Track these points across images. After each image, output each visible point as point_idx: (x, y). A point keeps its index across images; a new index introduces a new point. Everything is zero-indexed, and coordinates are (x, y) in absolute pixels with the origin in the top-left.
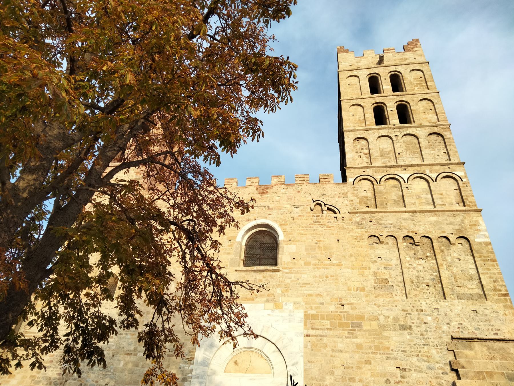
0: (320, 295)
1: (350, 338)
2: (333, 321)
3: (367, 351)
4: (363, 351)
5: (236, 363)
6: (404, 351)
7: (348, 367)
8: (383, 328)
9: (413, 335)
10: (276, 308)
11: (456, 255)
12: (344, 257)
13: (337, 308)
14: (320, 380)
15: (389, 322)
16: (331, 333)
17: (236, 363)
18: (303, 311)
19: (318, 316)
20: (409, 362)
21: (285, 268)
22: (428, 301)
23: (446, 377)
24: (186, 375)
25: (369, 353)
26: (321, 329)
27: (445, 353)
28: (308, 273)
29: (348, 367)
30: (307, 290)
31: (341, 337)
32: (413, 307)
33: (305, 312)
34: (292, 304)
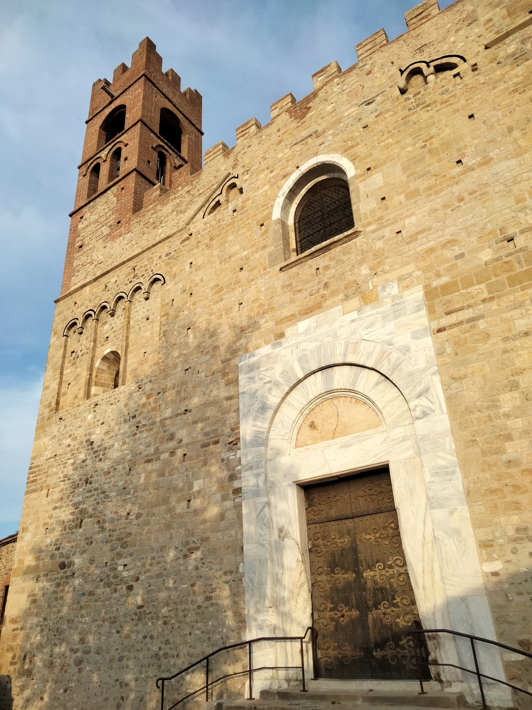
10: (366, 304)
12: (493, 141)
16: (493, 306)
26: (469, 306)
33: (425, 287)
34: (395, 284)
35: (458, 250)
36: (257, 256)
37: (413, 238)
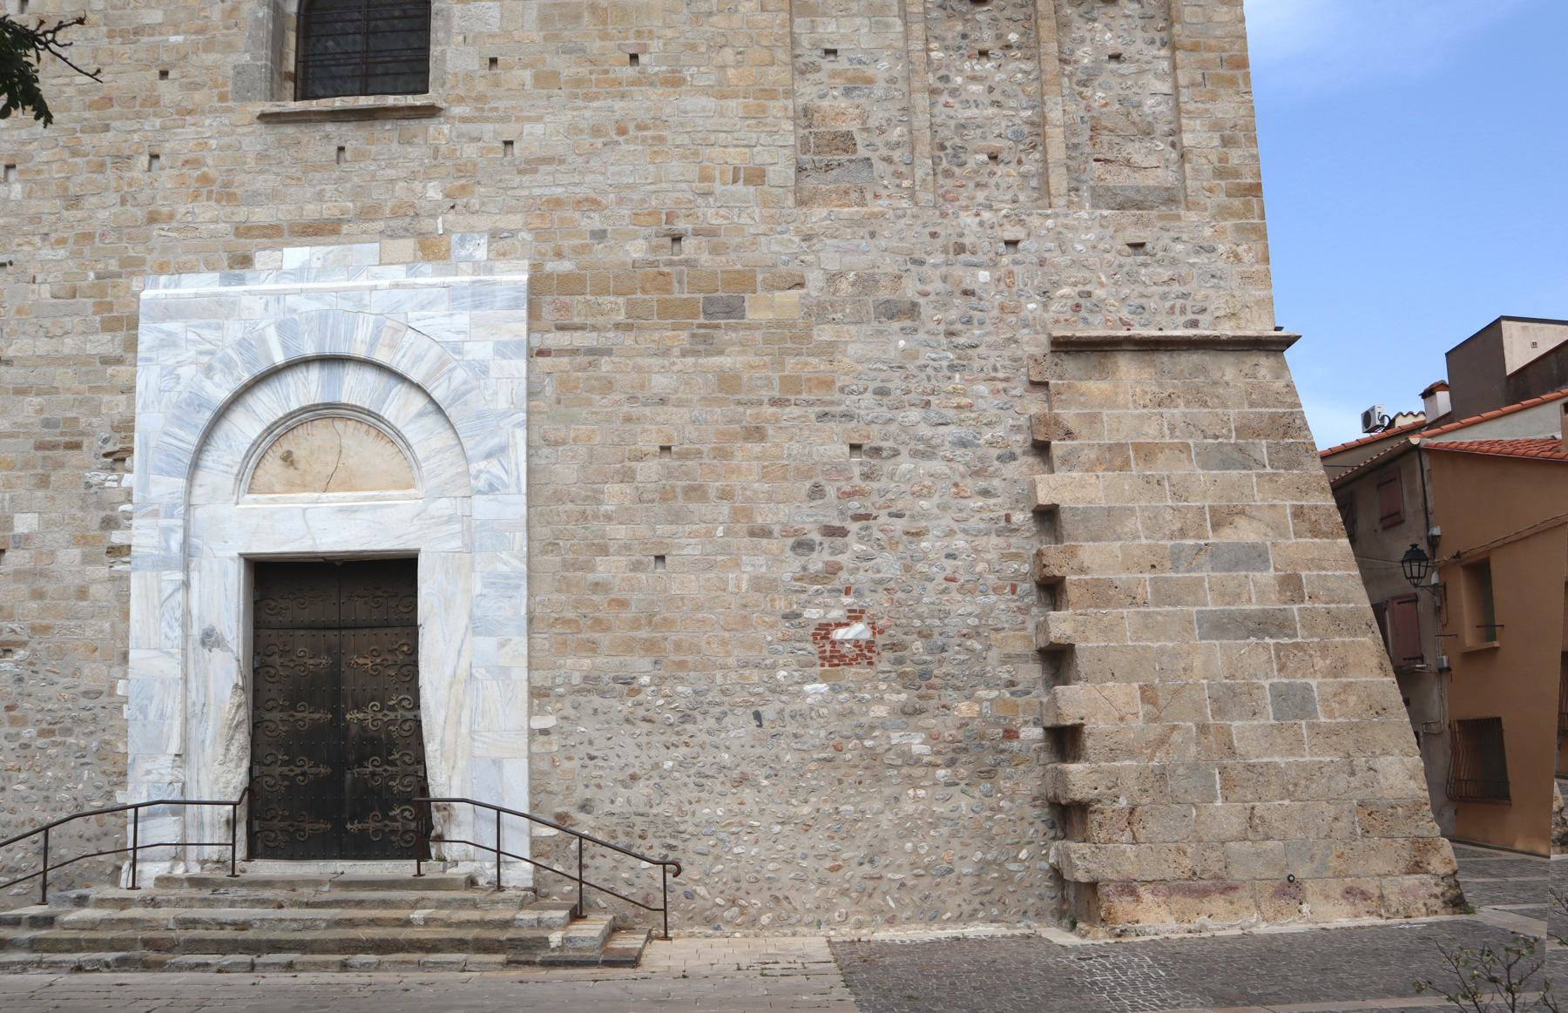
0: (594, 204)
1: (696, 353)
2: (639, 295)
3: (753, 397)
4: (742, 397)
5: (288, 459)
6: (882, 392)
7: (684, 455)
8: (819, 312)
9: (921, 335)
11: (1111, 41)
12: (693, 47)
13: (655, 249)
14: (586, 498)
15: (842, 294)
16: (628, 339)
17: (288, 459)
18: (526, 262)
19: (580, 280)
20: (893, 428)
21: (461, 100)
22: (986, 215)
23: (1010, 470)
24: (113, 509)
25: (760, 403)
26: (594, 328)
27: (1017, 392)
28: (547, 119)
29: (684, 455)
30: (542, 186)
31: (666, 353)
32: (934, 235)
34: (484, 241)
35: (596, 222)
36: (210, 58)
37: (531, 166)
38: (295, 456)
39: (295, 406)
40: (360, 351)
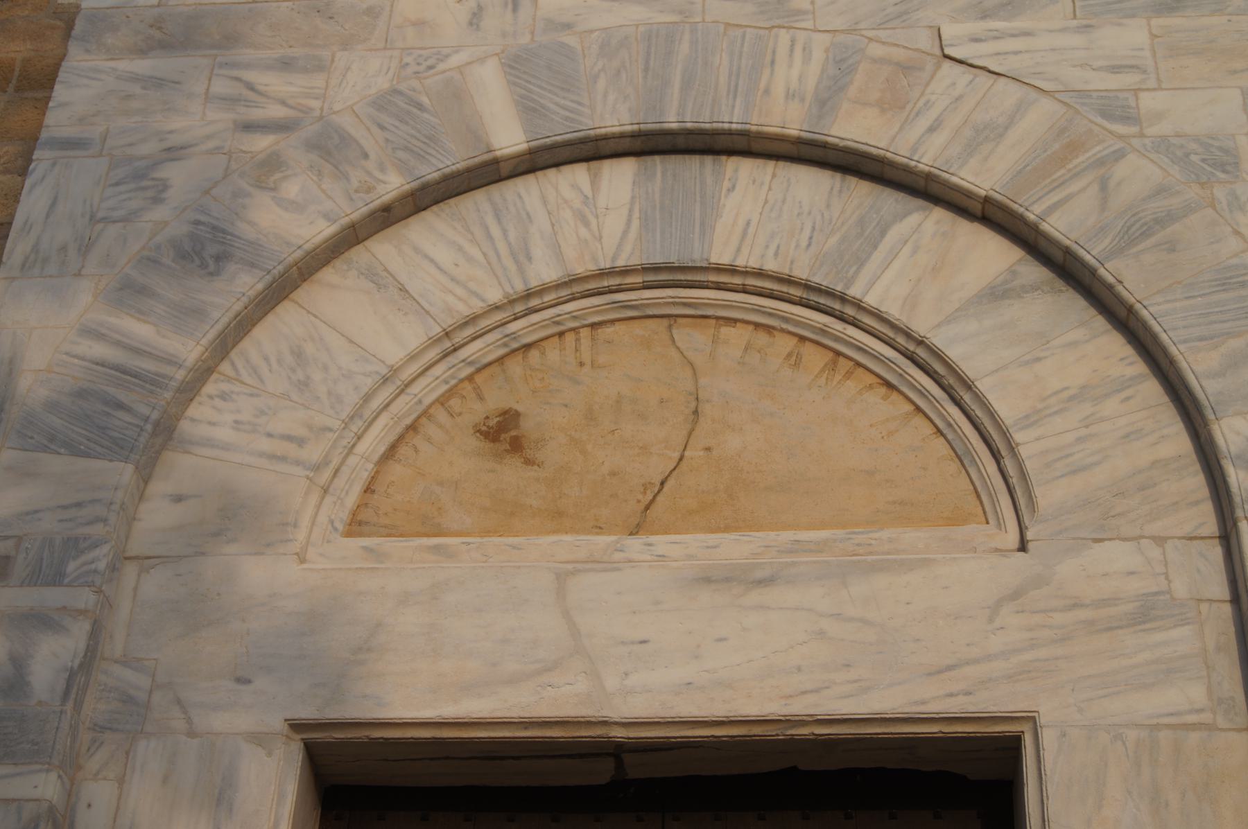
5: (503, 434)
17: (503, 434)
38: (527, 426)
39: (544, 271)
40: (785, 117)
